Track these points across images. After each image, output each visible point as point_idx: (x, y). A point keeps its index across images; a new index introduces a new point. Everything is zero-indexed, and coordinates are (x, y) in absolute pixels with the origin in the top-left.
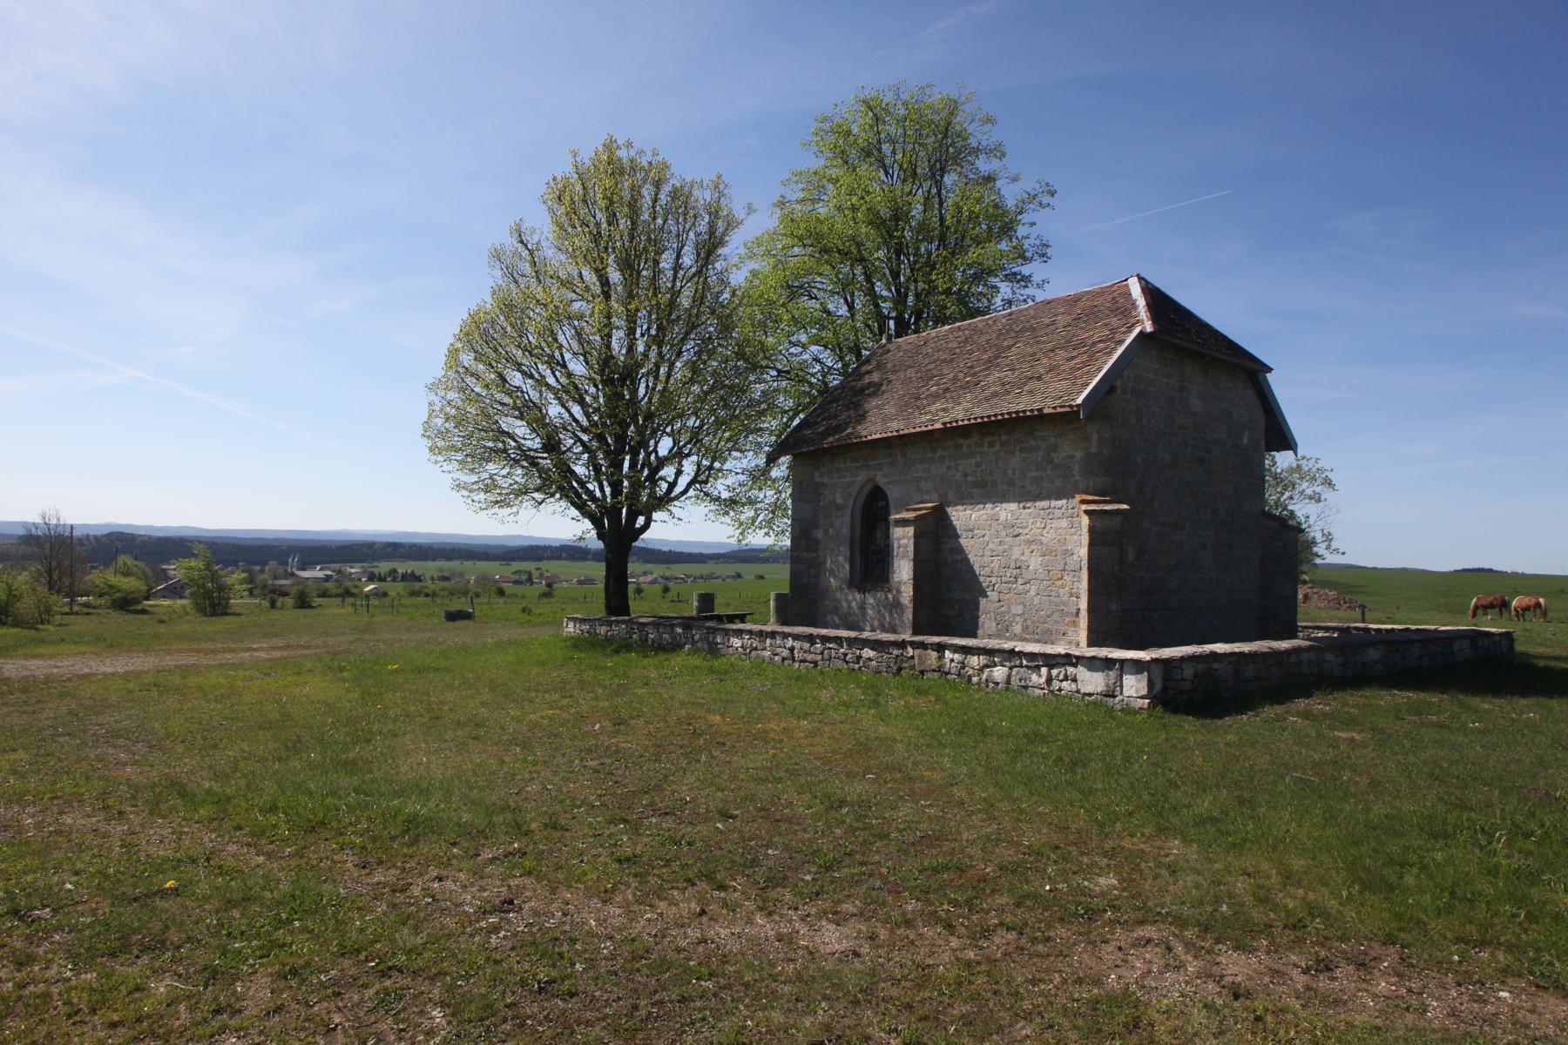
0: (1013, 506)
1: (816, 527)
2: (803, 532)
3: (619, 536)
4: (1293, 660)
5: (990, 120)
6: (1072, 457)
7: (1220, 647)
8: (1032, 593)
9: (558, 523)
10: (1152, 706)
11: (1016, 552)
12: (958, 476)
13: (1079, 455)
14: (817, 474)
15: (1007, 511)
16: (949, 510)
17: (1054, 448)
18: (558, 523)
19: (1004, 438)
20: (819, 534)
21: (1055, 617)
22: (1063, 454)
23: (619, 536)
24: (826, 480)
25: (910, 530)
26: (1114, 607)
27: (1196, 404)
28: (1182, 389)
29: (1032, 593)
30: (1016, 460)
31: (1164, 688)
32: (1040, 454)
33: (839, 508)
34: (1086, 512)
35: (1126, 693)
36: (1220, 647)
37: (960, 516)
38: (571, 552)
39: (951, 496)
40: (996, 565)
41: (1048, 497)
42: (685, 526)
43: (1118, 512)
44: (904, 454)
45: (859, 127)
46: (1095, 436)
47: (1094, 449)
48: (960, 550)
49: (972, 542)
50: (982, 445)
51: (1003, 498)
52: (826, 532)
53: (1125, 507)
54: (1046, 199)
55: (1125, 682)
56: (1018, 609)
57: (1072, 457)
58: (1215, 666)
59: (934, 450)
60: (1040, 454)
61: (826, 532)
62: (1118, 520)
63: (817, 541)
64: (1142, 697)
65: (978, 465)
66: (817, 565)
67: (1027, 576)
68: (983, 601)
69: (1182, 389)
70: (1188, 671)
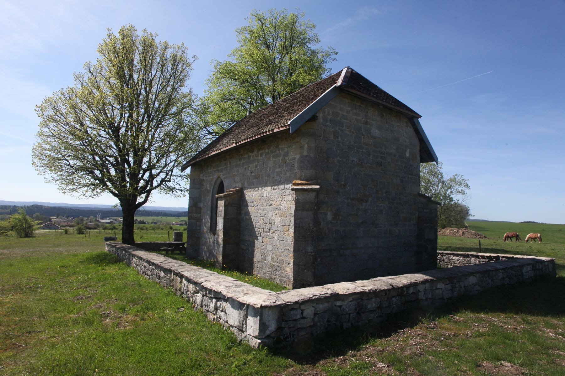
0: (269, 188)
1: (200, 201)
2: (217, 203)
3: (129, 206)
4: (411, 290)
5: (314, 26)
6: (295, 158)
7: (343, 287)
8: (276, 238)
9: (108, 200)
10: (263, 345)
11: (270, 214)
12: (249, 173)
13: (297, 157)
14: (202, 175)
15: (267, 191)
16: (245, 191)
17: (286, 155)
18: (108, 200)
19: (267, 151)
20: (201, 205)
21: (286, 252)
22: (291, 157)
23: (129, 206)
24: (205, 178)
25: (223, 202)
26: (309, 249)
27: (376, 132)
28: (366, 123)
29: (276, 238)
30: (271, 163)
31: (279, 328)
32: (281, 158)
33: (208, 191)
34: (292, 190)
35: (248, 332)
36: (343, 287)
37: (250, 195)
38: (106, 213)
39: (246, 185)
40: (261, 222)
41: (284, 183)
42: (158, 200)
43: (312, 190)
44: (230, 163)
45: (255, 26)
46: (306, 146)
47: (305, 154)
48: (248, 213)
49: (253, 209)
50: (258, 156)
51: (266, 185)
52: (204, 204)
53: (318, 187)
54: (334, 56)
55: (248, 321)
56: (269, 248)
57: (295, 158)
58: (339, 303)
59: (240, 160)
60: (281, 158)
61: (204, 204)
62: (313, 195)
63: (200, 208)
64: (256, 337)
65: (256, 167)
66: (200, 220)
67: (274, 228)
68: (256, 242)
69: (366, 123)
70: (309, 311)
